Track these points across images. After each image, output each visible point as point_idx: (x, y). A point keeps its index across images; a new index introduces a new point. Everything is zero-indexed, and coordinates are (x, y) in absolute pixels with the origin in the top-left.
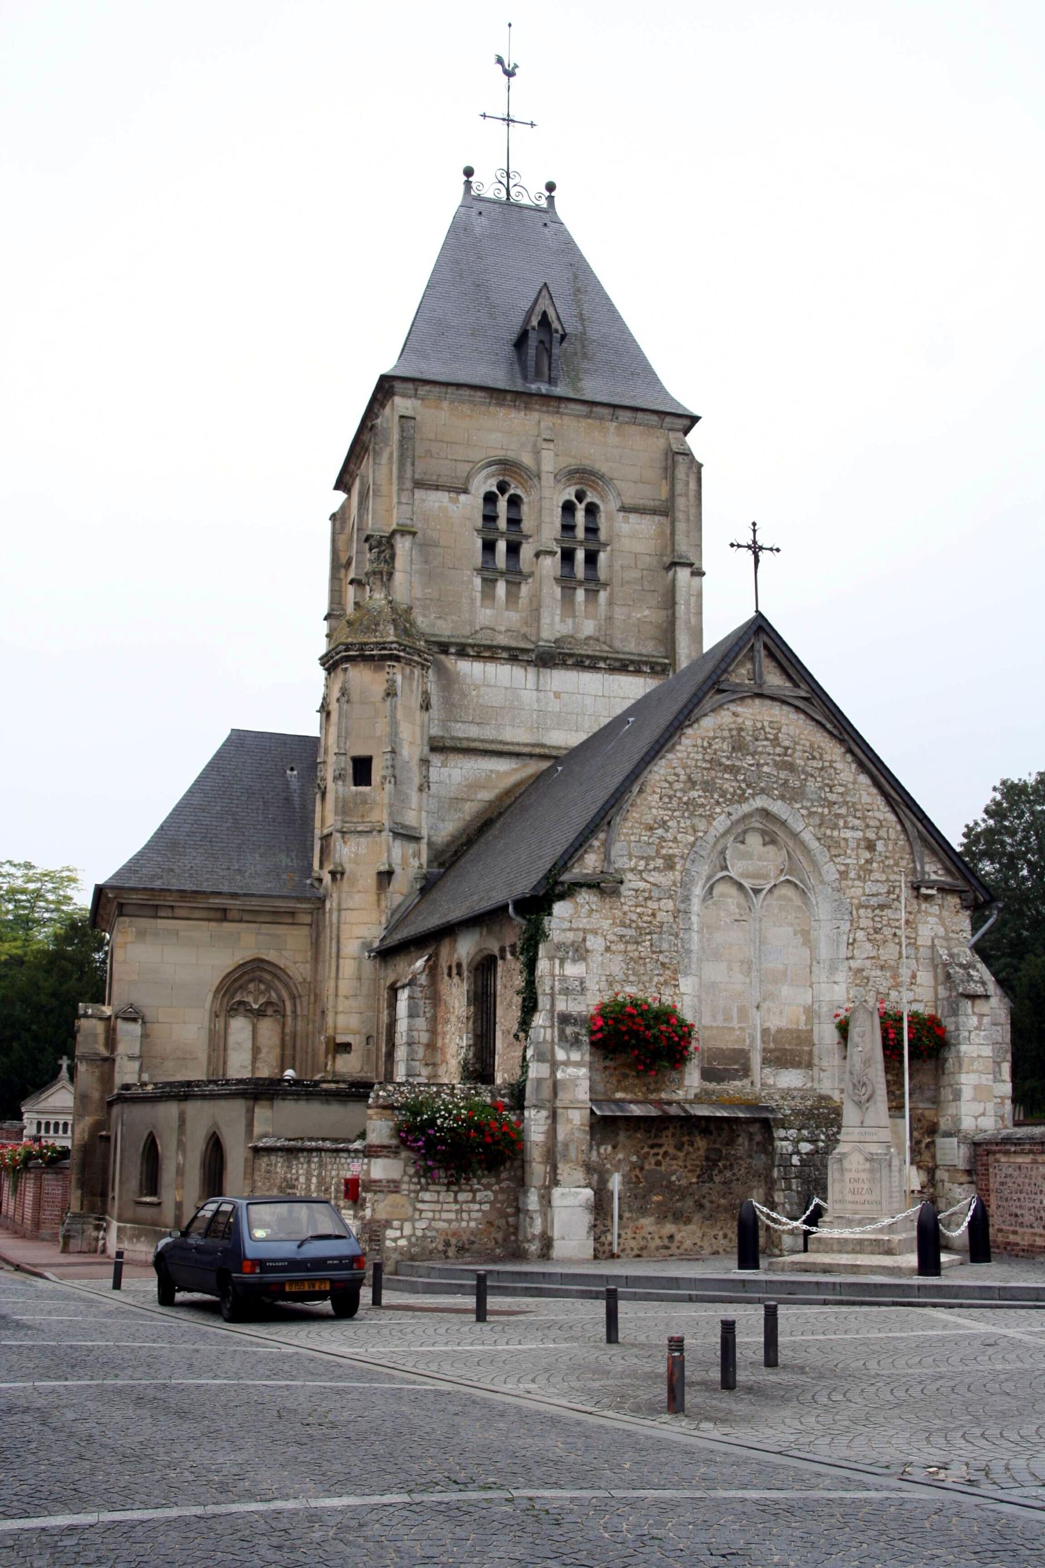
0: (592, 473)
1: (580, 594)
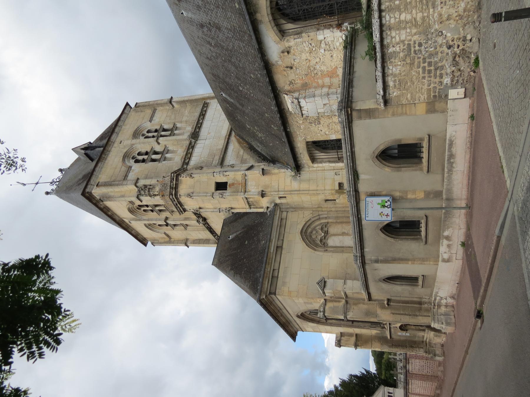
0: (136, 130)
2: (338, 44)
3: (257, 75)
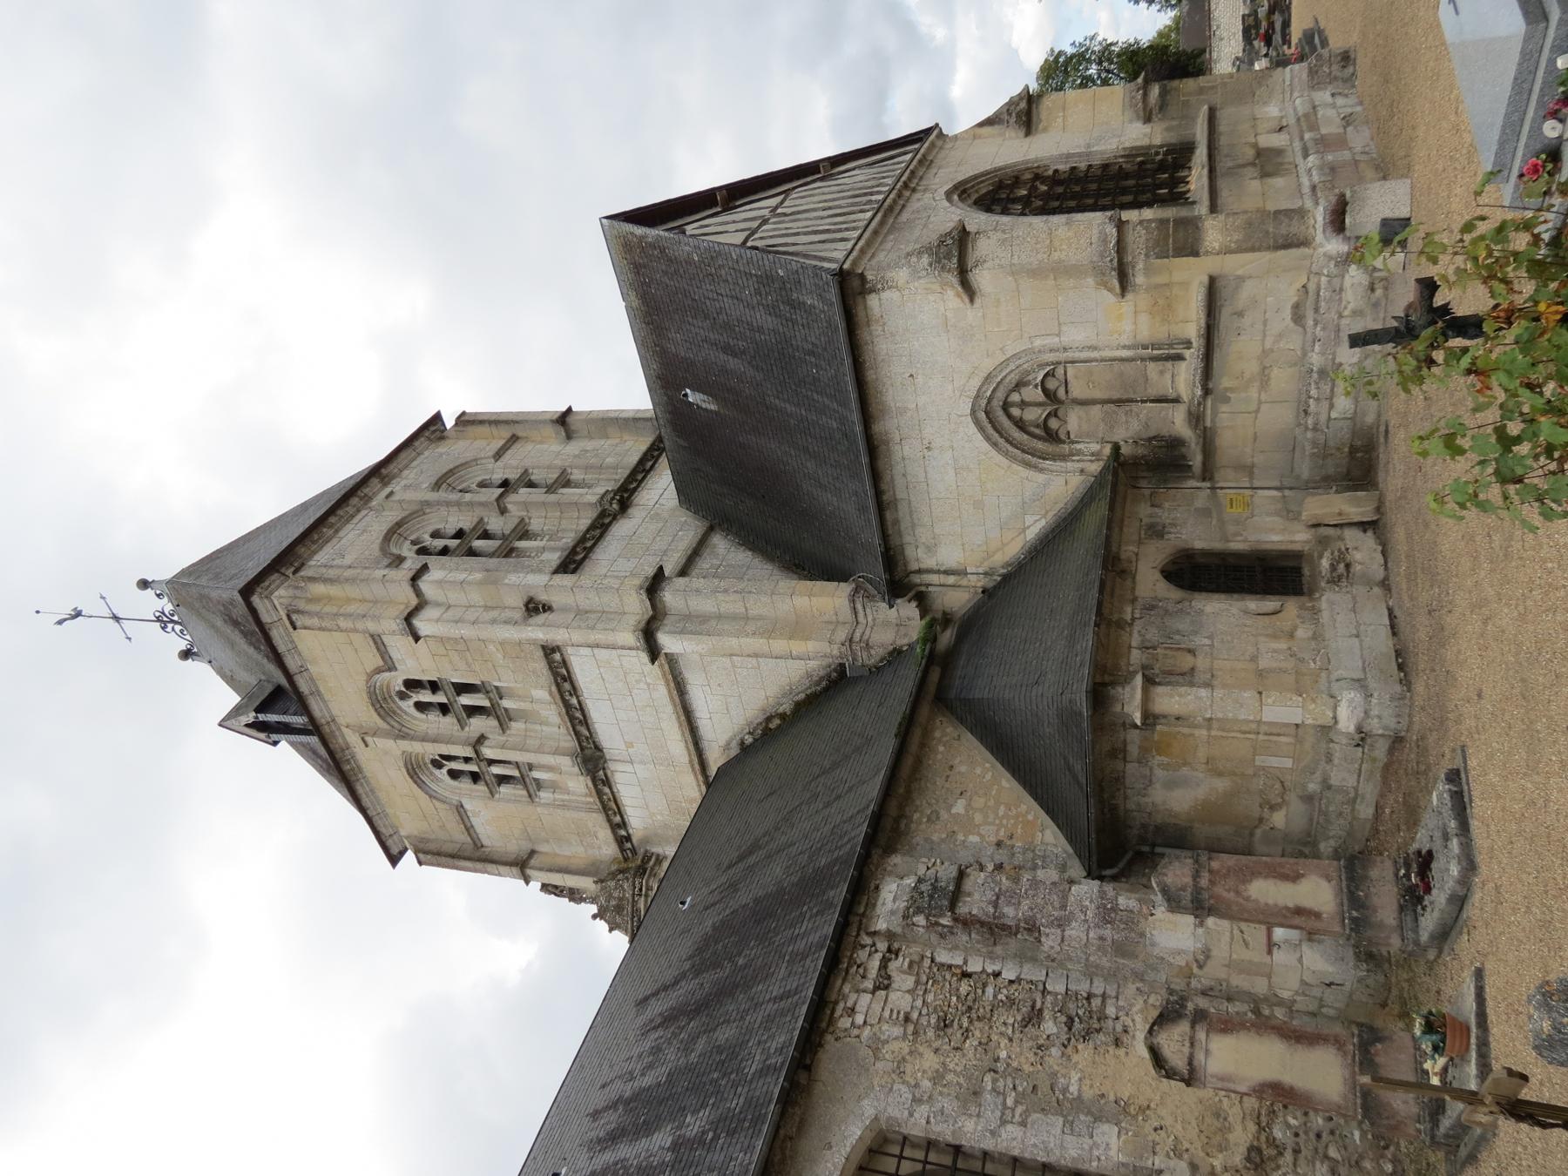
1: (506, 703)
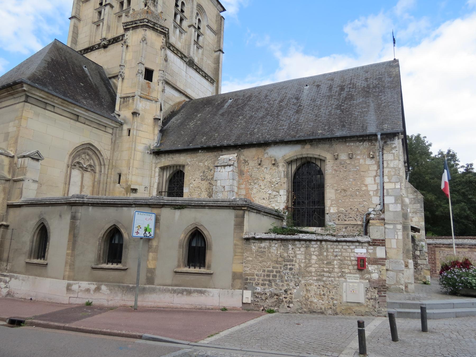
2: (273, 205)
3: (257, 134)
